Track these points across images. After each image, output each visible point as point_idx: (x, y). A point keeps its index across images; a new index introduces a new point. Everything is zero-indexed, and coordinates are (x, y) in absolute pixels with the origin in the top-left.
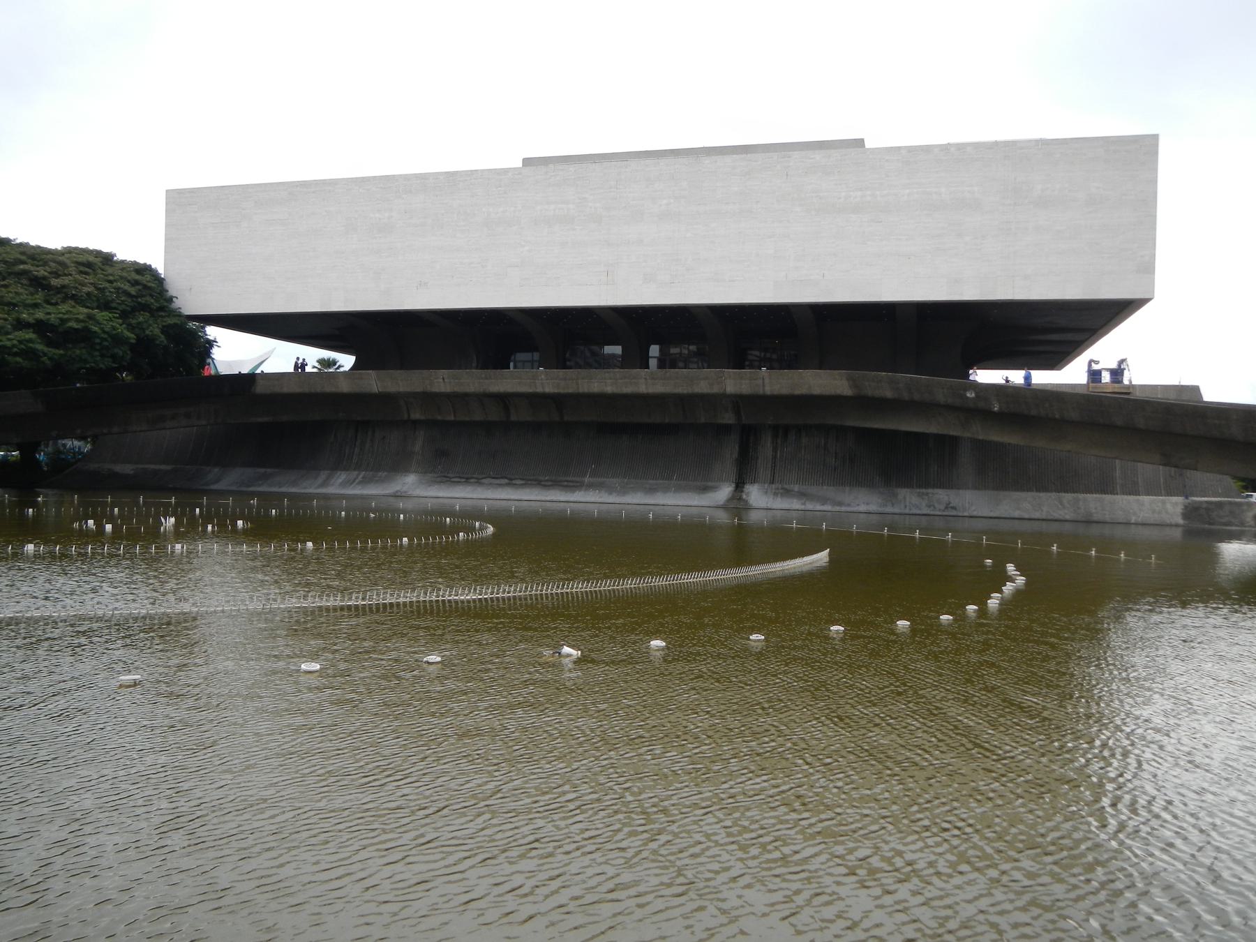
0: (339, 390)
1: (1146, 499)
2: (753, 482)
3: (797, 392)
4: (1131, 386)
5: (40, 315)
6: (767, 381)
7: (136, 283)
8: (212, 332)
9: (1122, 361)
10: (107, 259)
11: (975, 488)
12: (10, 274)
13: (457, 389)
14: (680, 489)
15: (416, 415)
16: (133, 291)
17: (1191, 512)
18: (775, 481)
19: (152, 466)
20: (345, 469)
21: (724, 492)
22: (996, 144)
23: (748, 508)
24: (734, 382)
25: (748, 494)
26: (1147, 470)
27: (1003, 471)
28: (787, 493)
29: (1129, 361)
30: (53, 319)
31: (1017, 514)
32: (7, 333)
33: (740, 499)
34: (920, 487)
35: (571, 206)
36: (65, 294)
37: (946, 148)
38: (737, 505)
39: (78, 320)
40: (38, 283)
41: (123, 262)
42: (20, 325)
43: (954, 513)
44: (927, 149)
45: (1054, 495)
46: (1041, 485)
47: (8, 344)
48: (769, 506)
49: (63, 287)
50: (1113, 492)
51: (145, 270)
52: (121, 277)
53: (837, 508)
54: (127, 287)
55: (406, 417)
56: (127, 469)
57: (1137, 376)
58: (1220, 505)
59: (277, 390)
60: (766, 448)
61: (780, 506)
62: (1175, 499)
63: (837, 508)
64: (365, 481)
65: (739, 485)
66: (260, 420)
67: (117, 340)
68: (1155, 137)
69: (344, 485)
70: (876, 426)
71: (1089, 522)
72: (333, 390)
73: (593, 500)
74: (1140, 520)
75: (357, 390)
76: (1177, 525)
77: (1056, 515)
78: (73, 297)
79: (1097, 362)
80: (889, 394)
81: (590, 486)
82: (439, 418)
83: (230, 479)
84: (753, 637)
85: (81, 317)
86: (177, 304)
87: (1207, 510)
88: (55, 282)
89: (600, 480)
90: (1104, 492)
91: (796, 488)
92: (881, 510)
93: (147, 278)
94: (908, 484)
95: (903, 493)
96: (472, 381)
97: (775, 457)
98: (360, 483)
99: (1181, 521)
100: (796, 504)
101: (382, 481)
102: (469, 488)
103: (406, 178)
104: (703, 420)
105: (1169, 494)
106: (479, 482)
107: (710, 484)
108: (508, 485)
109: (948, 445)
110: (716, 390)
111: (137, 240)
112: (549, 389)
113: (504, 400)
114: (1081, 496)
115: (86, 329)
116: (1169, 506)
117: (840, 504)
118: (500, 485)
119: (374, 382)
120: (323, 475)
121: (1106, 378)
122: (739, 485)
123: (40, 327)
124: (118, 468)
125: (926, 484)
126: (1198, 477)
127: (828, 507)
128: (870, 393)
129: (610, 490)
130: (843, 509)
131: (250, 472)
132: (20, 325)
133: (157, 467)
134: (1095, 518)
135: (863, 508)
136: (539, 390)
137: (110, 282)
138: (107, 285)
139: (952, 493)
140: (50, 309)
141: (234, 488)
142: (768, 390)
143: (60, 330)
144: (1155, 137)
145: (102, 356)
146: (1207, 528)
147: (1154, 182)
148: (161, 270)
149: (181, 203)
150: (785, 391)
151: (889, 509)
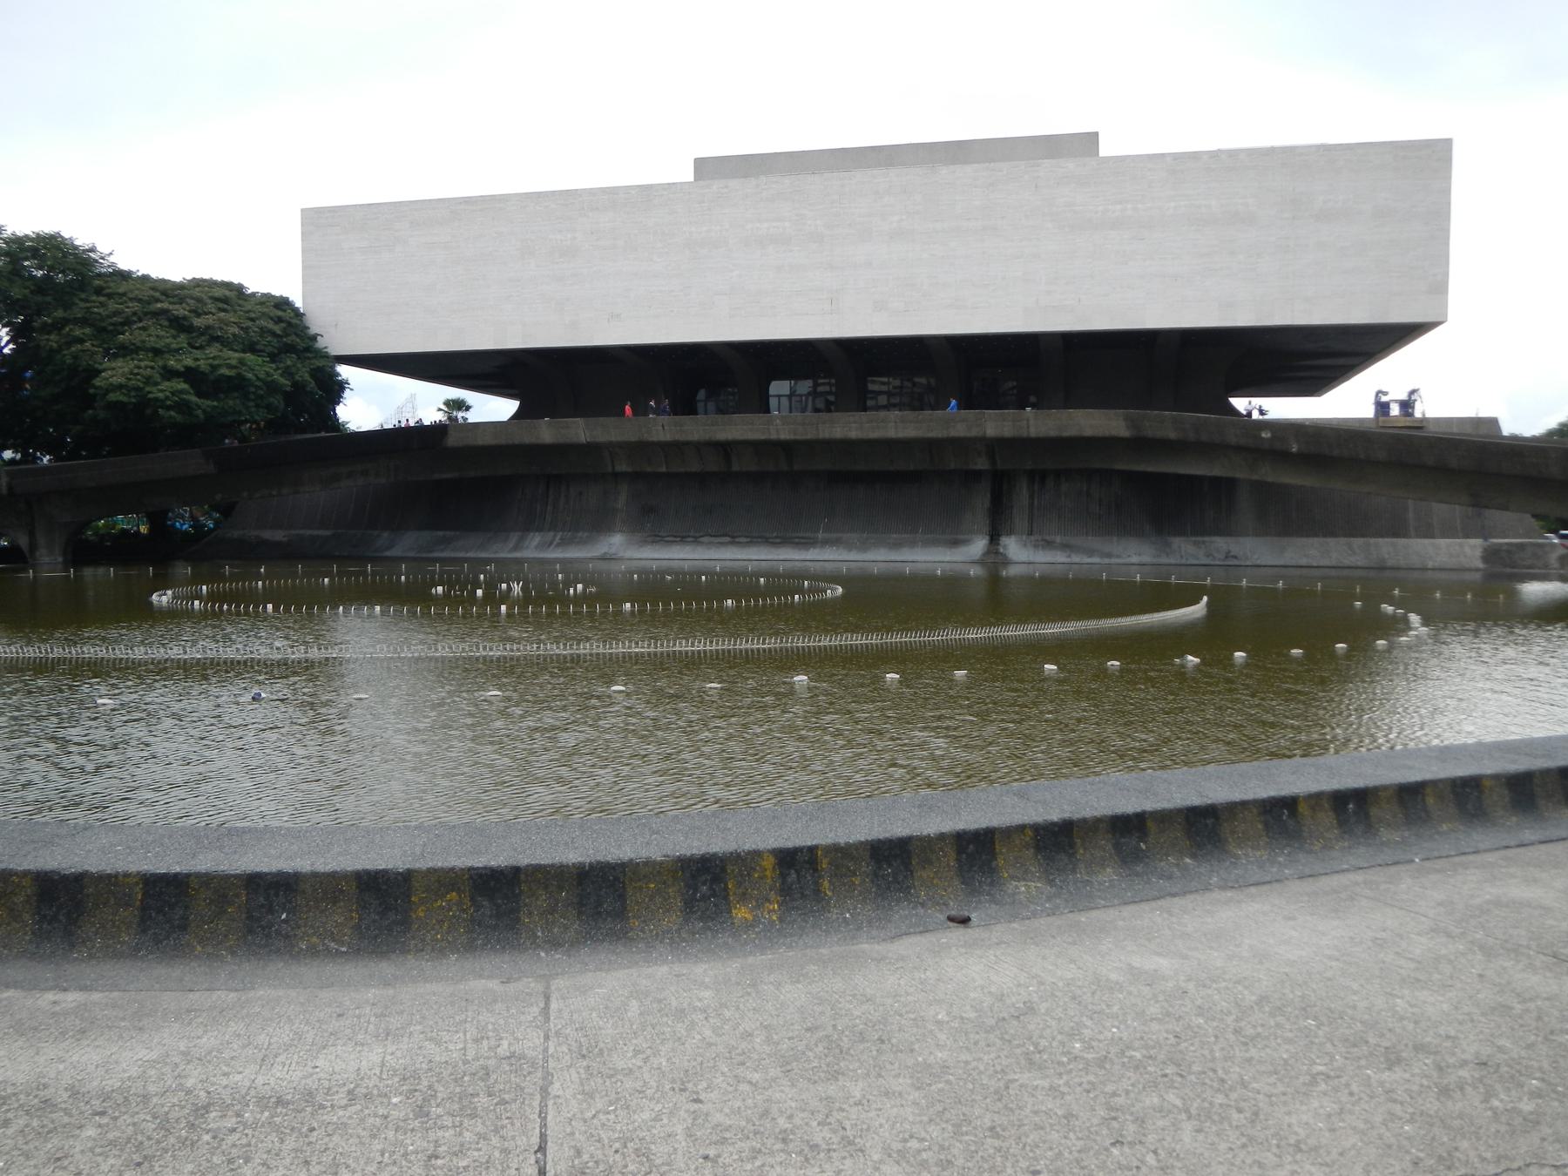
0: (540, 442)
1: (1443, 542)
2: (1010, 533)
3: (1065, 434)
4: (1424, 419)
5: (189, 362)
6: (1032, 422)
7: (279, 320)
8: (344, 371)
9: (1413, 392)
10: (239, 289)
11: (1258, 533)
12: (146, 314)
14: (928, 543)
15: (622, 467)
16: (277, 329)
17: (1491, 555)
18: (1035, 533)
19: (309, 532)
20: (539, 529)
21: (978, 546)
22: (1272, 151)
23: (1007, 562)
24: (995, 424)
25: (1005, 547)
26: (1440, 510)
27: (1288, 515)
28: (1049, 545)
29: (1422, 392)
30: (203, 365)
31: (1304, 562)
32: (156, 384)
33: (997, 553)
34: (1196, 533)
35: (787, 224)
37: (1215, 155)
38: (994, 559)
39: (231, 367)
40: (179, 325)
41: (254, 294)
42: (169, 374)
43: (1236, 562)
44: (1195, 156)
45: (1343, 540)
46: (1327, 530)
47: (161, 395)
48: (1031, 559)
49: (208, 327)
50: (1406, 535)
51: (283, 304)
52: (264, 314)
53: (1107, 561)
54: (271, 325)
55: (610, 469)
56: (279, 535)
57: (1431, 408)
58: (1521, 547)
59: (471, 442)
60: (1022, 495)
61: (1043, 560)
62: (1473, 541)
63: (1107, 561)
64: (564, 543)
65: (994, 538)
66: (445, 476)
67: (272, 387)
68: (1446, 144)
69: (540, 547)
70: (1150, 469)
71: (1382, 568)
72: (533, 440)
73: (831, 557)
74: (1437, 565)
75: (561, 440)
76: (1477, 570)
77: (1347, 562)
78: (217, 339)
79: (1385, 394)
80: (1172, 435)
81: (826, 543)
82: (649, 469)
83: (406, 544)
84: (1238, 654)
85: (234, 362)
86: (321, 343)
87: (1509, 552)
88: (197, 322)
89: (835, 535)
90: (1396, 535)
91: (1058, 539)
92: (1155, 561)
93: (288, 315)
94: (1182, 533)
95: (1177, 541)
96: (662, 427)
97: (1031, 505)
98: (558, 545)
99: (1481, 566)
100: (1060, 557)
101: (583, 542)
102: (688, 548)
103: (591, 192)
104: (952, 466)
105: (1467, 537)
106: (696, 541)
107: (961, 537)
108: (732, 543)
109: (1224, 488)
110: (974, 433)
111: (271, 269)
113: (725, 449)
114: (1372, 540)
115: (240, 377)
116: (1467, 550)
117: (1109, 555)
118: (722, 544)
119: (546, 431)
120: (514, 537)
121: (1395, 410)
122: (994, 538)
123: (190, 375)
124: (267, 535)
125: (1202, 534)
126: (1495, 516)
127: (1096, 560)
128: (1150, 433)
129: (850, 547)
130: (1114, 560)
131: (426, 536)
132: (169, 374)
133: (316, 532)
134: (1390, 563)
135: (1135, 559)
136: (774, 436)
137: (253, 320)
138: (250, 324)
139: (1229, 539)
140: (198, 354)
141: (412, 554)
142: (1033, 432)
143: (212, 377)
144: (1446, 144)
145: (257, 406)
146: (1506, 568)
147: (1446, 192)
148: (299, 303)
149: (321, 225)
150: (1053, 433)
151: (1164, 560)
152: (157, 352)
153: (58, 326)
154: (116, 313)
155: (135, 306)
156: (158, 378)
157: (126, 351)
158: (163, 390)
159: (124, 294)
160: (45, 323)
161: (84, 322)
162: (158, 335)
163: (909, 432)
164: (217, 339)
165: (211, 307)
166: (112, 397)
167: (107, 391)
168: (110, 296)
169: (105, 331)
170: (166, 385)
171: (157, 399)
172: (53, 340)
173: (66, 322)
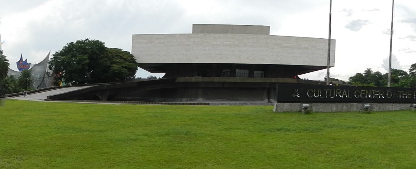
2: (271, 98)
13: (219, 81)
32: (121, 69)
36: (126, 60)
39: (132, 66)
42: (123, 67)
49: (126, 58)
51: (129, 53)
54: (131, 58)
78: (127, 61)
96: (200, 79)
101: (194, 100)
112: (239, 81)
120: (179, 99)
123: (126, 67)
136: (237, 81)
149: (136, 38)
152: (119, 63)
153: (102, 58)
154: (111, 56)
155: (114, 54)
156: (122, 68)
157: (114, 63)
158: (124, 70)
159: (111, 52)
160: (100, 58)
161: (106, 57)
162: (118, 60)
163: (261, 81)
164: (127, 61)
165: (123, 54)
166: (117, 71)
167: (115, 70)
168: (109, 52)
169: (110, 59)
170: (123, 70)
171: (123, 72)
172: (102, 61)
173: (104, 57)
